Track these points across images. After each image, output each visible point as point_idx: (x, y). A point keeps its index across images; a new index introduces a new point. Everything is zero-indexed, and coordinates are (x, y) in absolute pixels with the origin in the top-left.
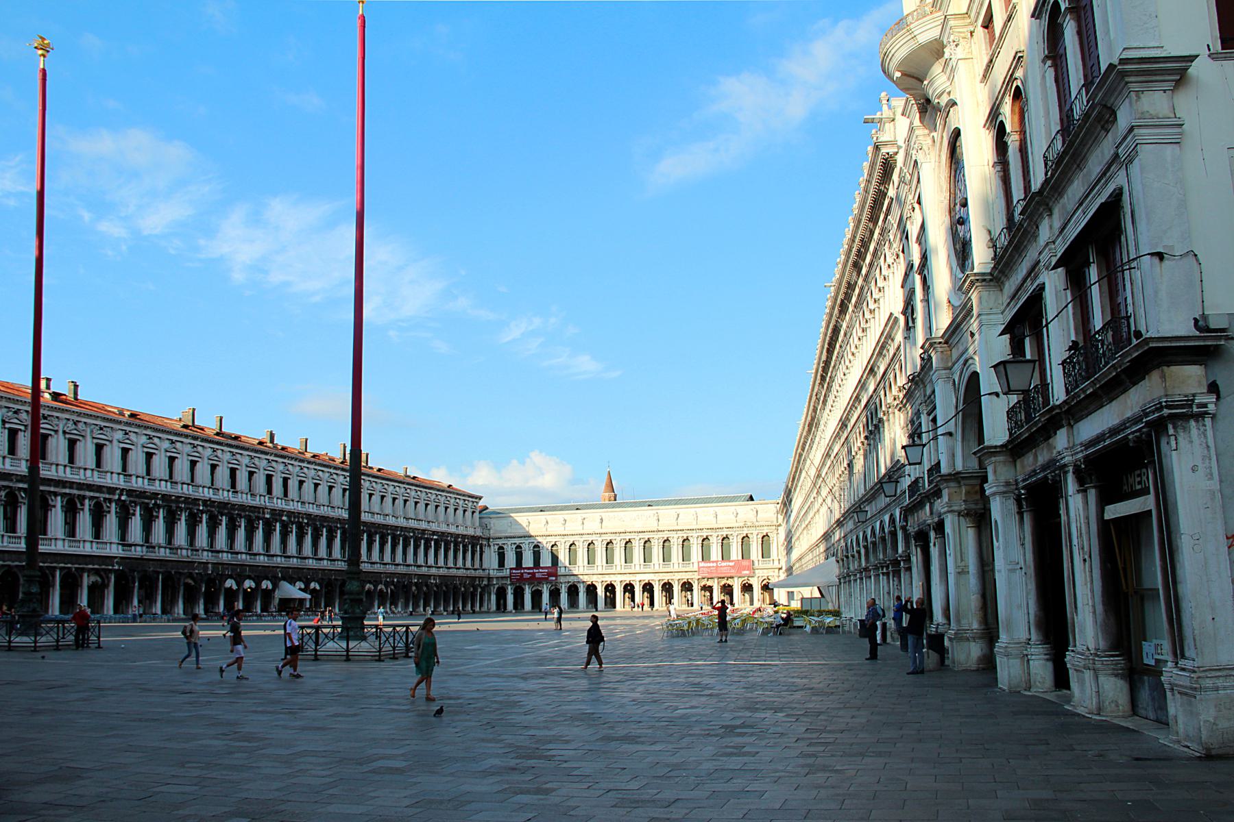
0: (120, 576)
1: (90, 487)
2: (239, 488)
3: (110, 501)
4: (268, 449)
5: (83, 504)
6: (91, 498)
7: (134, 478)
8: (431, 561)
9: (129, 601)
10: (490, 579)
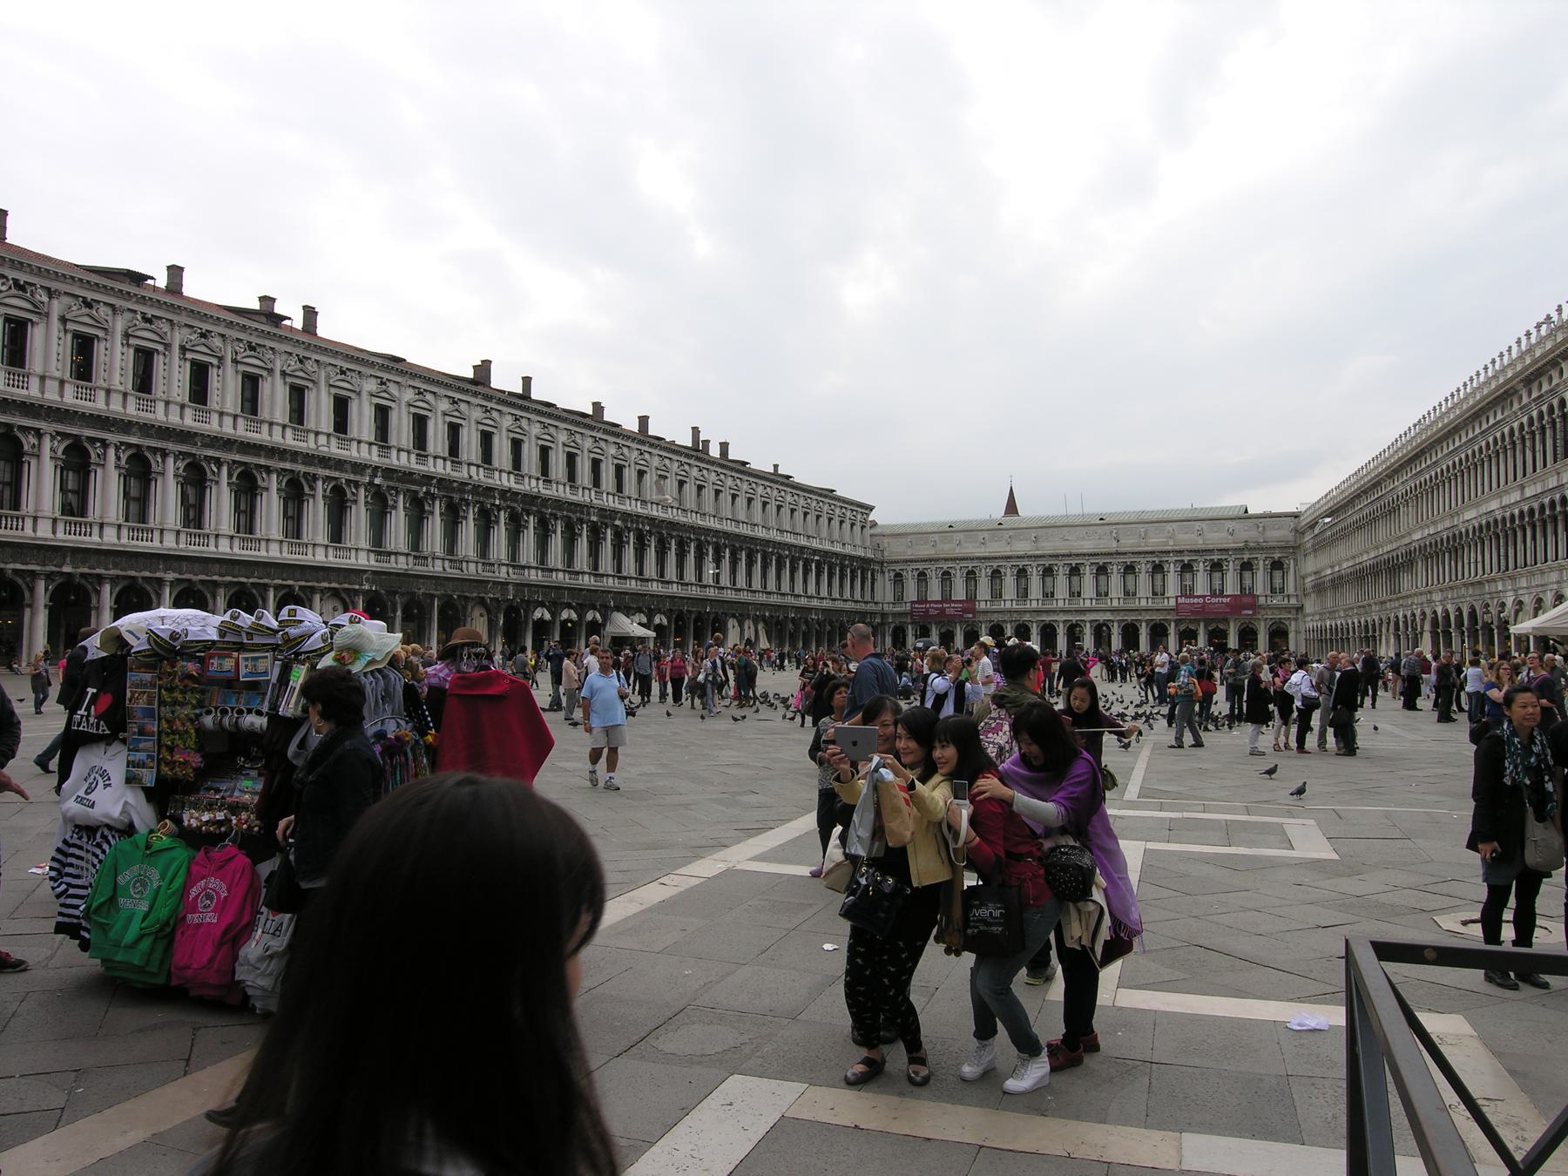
1: (325, 461)
2: (553, 476)
3: (357, 484)
4: (593, 421)
5: (312, 488)
6: (327, 479)
7: (394, 453)
8: (812, 589)
10: (884, 615)
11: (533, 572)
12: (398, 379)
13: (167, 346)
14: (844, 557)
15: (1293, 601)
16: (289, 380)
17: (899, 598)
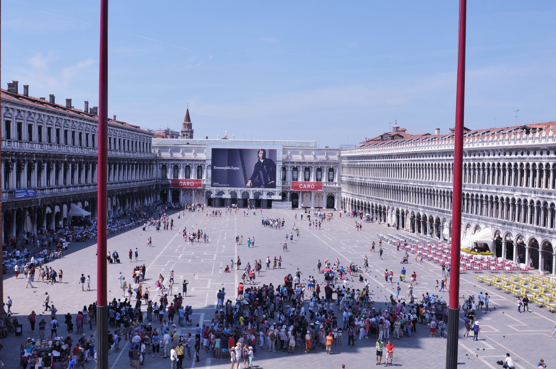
11: (47, 191)
15: (337, 185)
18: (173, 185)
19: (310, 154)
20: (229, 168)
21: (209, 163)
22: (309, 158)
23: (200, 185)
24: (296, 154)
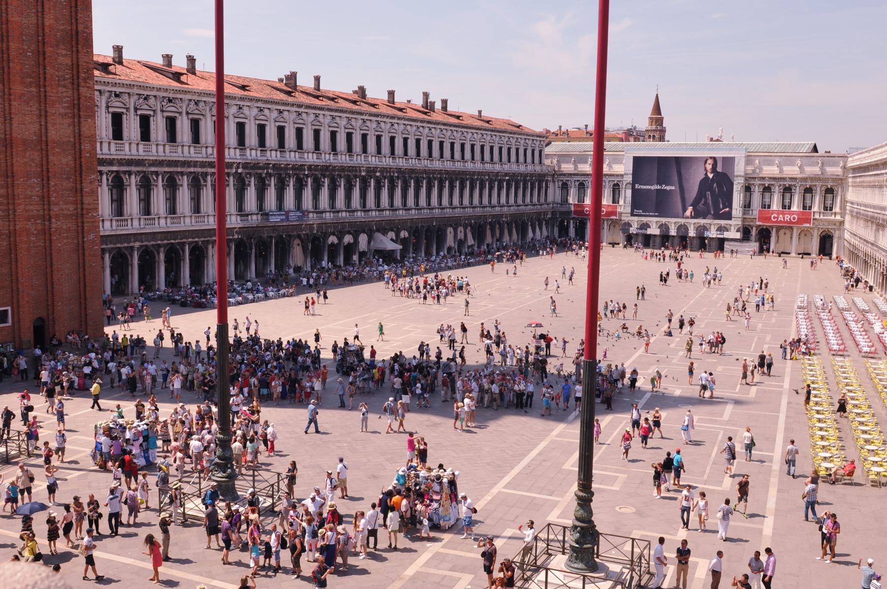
0: (240, 244)
5: (205, 181)
7: (248, 151)
9: (247, 266)
11: (328, 214)
12: (249, 104)
13: (128, 109)
14: (526, 175)
15: (838, 217)
16: (191, 116)
17: (565, 201)
18: (576, 212)
19: (792, 164)
20: (659, 187)
21: (629, 179)
22: (791, 171)
23: (614, 213)
24: (769, 165)
